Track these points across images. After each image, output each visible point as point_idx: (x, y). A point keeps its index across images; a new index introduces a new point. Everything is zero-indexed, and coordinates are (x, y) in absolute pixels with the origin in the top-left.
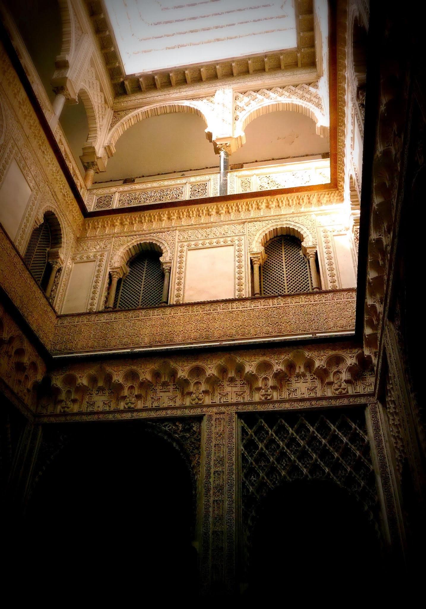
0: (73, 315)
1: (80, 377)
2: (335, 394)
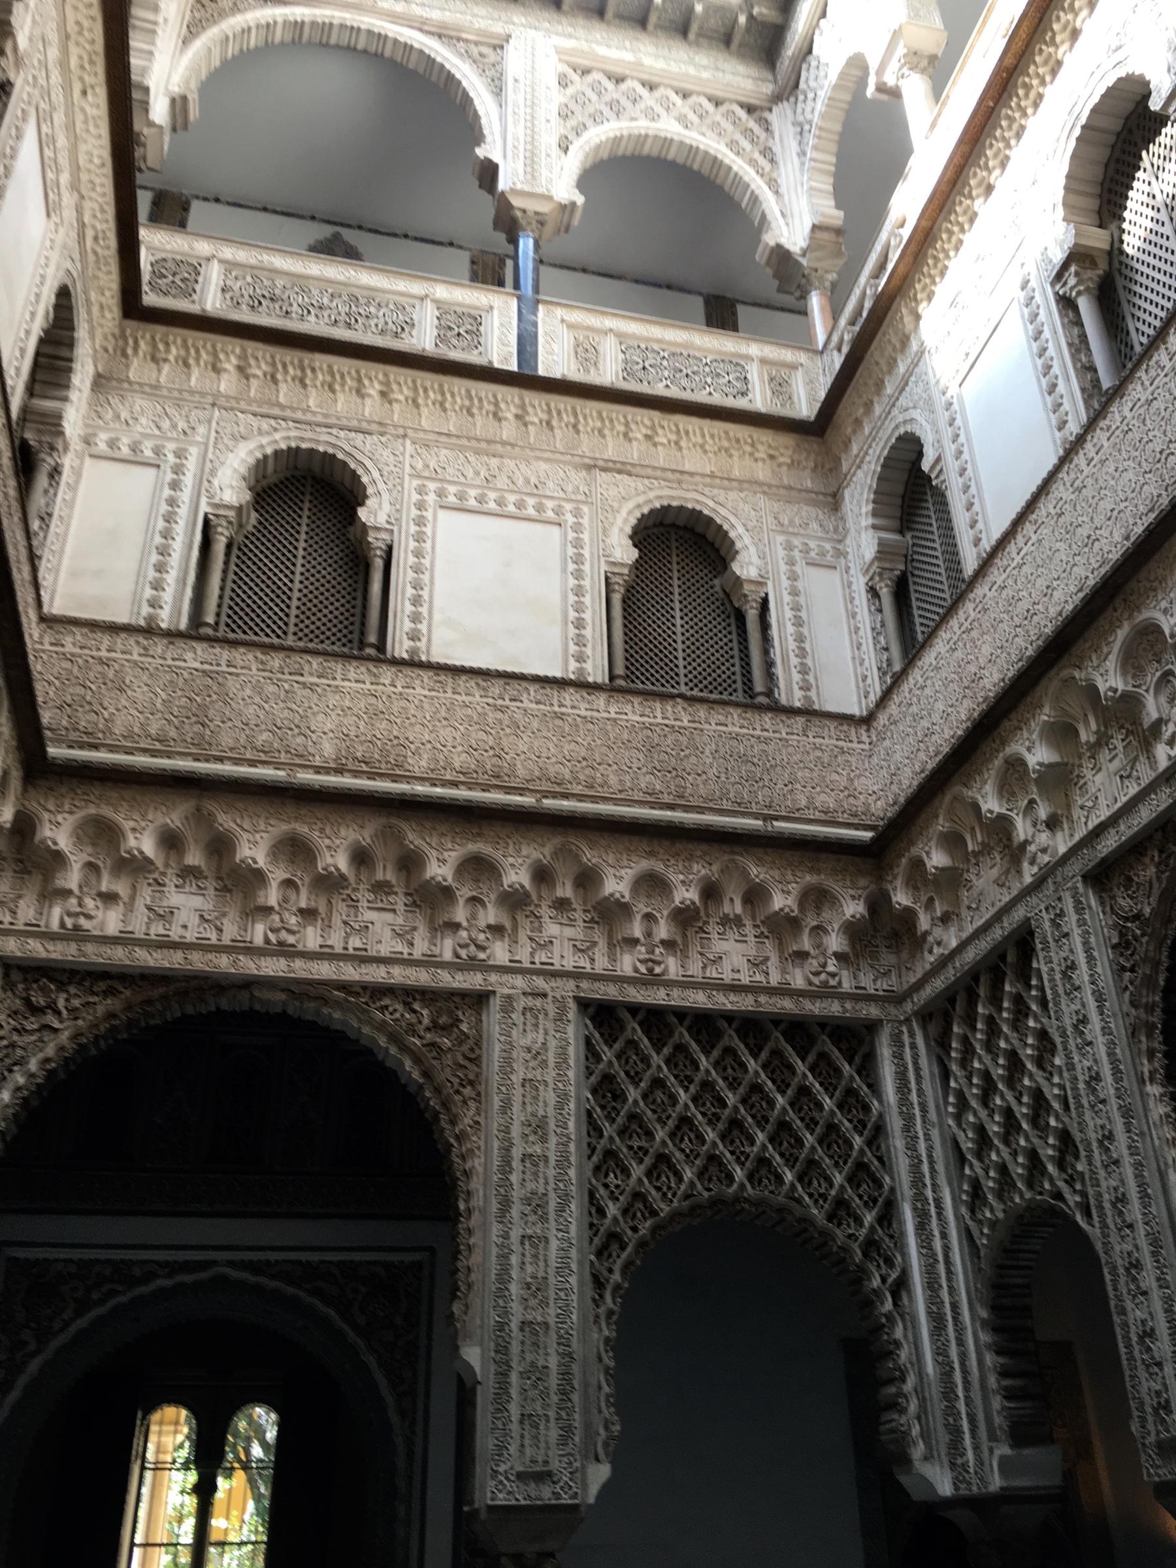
0: (93, 625)
1: (134, 830)
2: (811, 983)
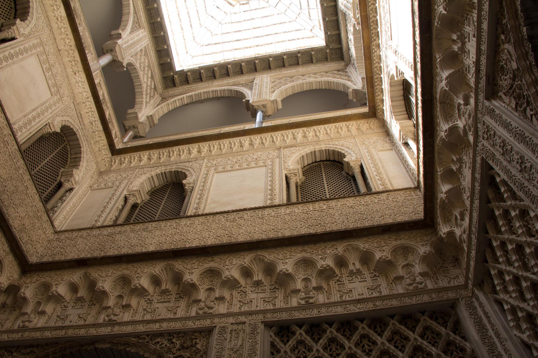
1: (56, 284)
2: (407, 290)
